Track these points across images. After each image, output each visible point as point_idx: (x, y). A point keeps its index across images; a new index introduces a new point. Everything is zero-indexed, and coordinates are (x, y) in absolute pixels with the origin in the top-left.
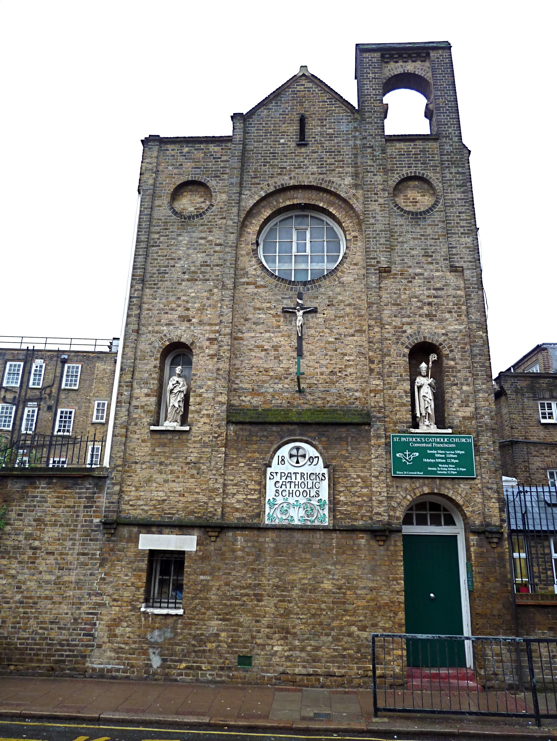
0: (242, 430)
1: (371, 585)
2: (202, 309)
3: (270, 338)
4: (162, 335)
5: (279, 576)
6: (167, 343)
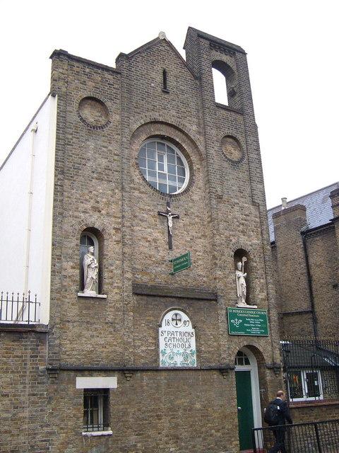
0: (142, 299)
1: (220, 403)
2: (108, 204)
3: (151, 233)
4: (79, 220)
5: (171, 402)
6: (85, 227)
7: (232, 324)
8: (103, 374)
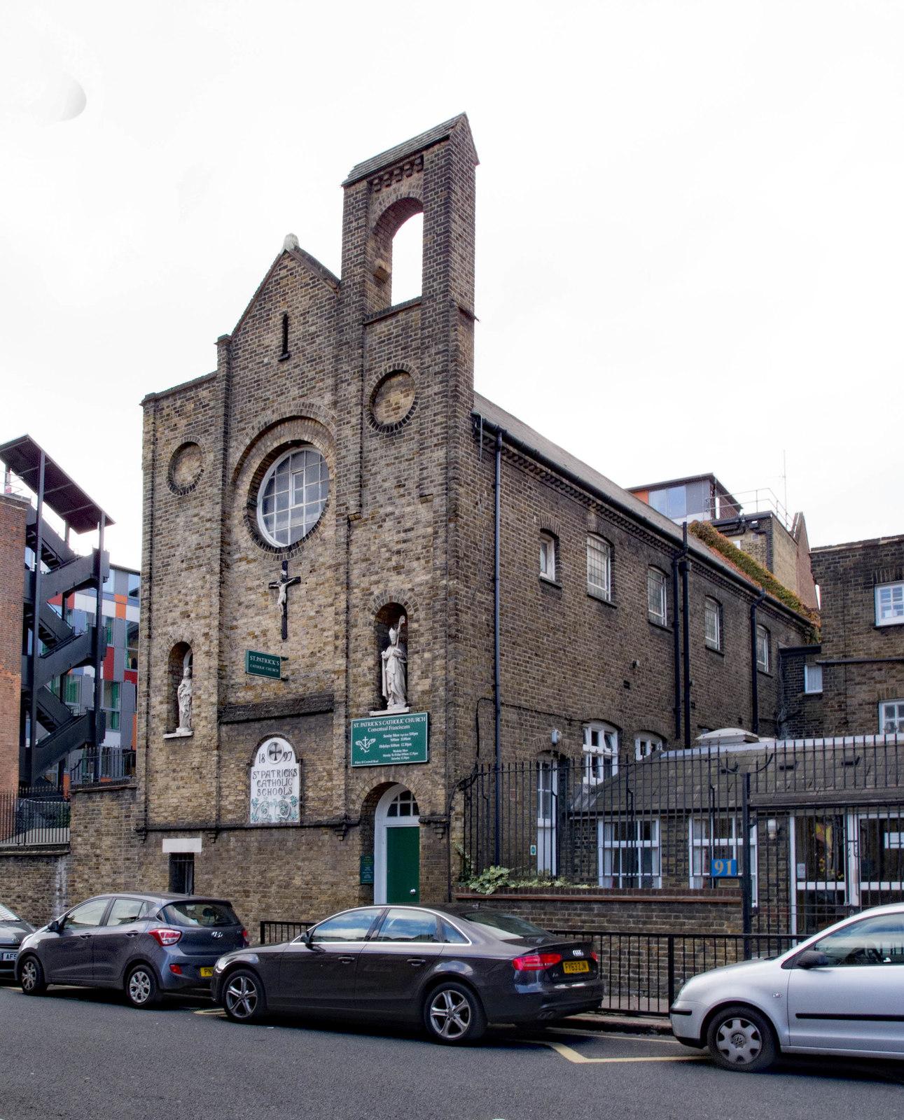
0: (231, 729)
1: (332, 880)
2: (197, 602)
3: (260, 623)
4: (166, 637)
5: (262, 873)
6: (173, 645)
7: (356, 748)
8: (187, 834)
